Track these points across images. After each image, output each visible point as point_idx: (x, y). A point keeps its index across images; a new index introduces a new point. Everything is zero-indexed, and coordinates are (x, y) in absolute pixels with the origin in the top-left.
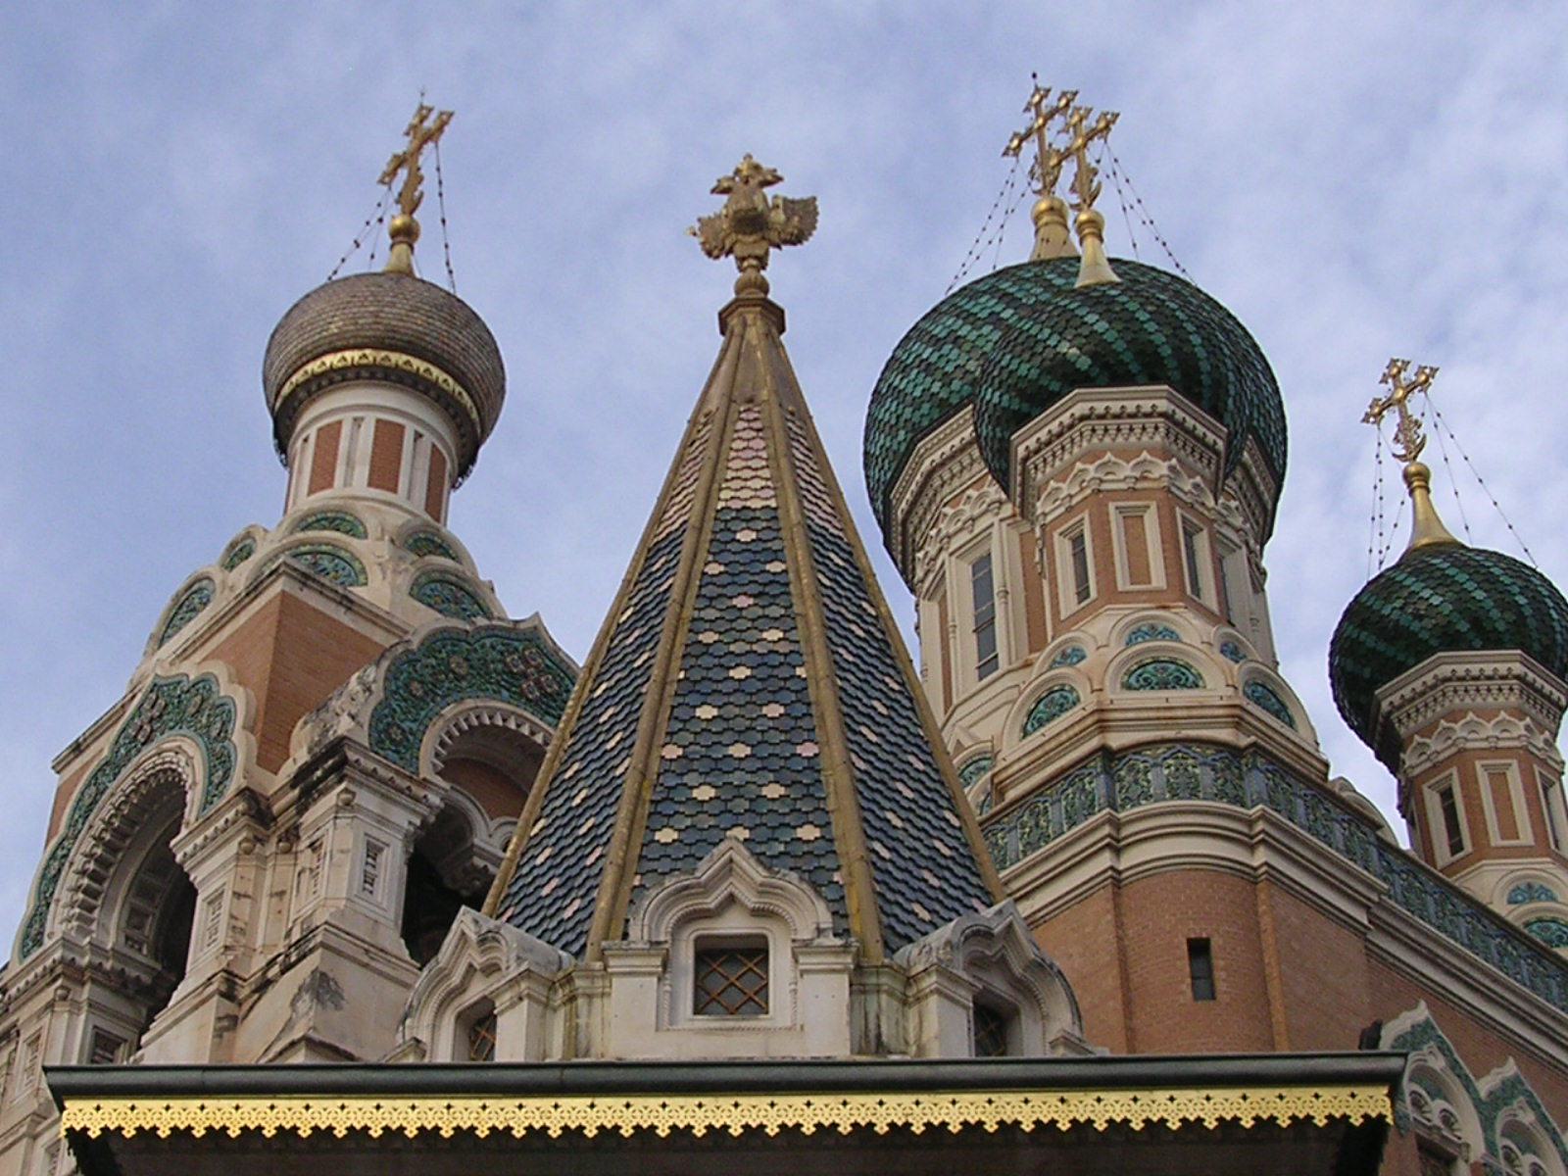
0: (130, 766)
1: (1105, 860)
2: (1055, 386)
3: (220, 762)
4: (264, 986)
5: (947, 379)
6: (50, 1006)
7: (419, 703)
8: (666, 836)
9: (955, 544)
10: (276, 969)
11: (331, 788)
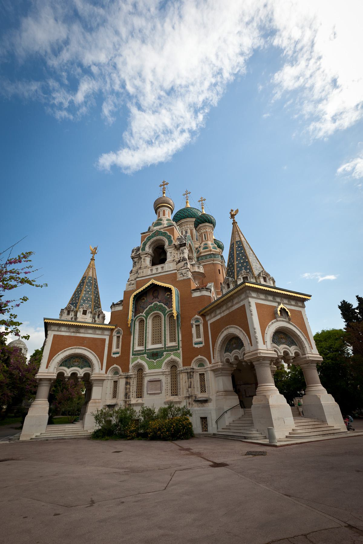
0: (156, 237)
1: (212, 262)
2: (205, 222)
3: (170, 242)
4: (179, 262)
5: (185, 215)
6: (146, 256)
9: (185, 229)
10: (181, 261)
11: (183, 247)
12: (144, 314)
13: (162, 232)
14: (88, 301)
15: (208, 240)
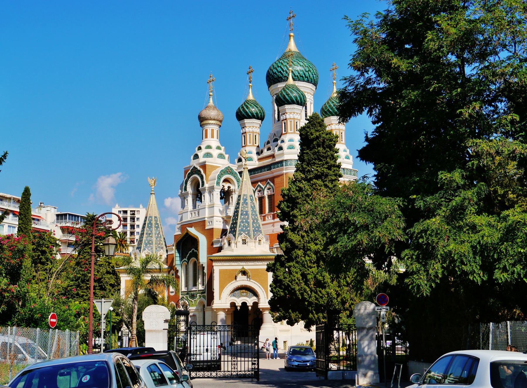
7: (219, 179)
8: (240, 229)
12: (186, 259)
13: (197, 169)
14: (150, 244)
15: (286, 134)
